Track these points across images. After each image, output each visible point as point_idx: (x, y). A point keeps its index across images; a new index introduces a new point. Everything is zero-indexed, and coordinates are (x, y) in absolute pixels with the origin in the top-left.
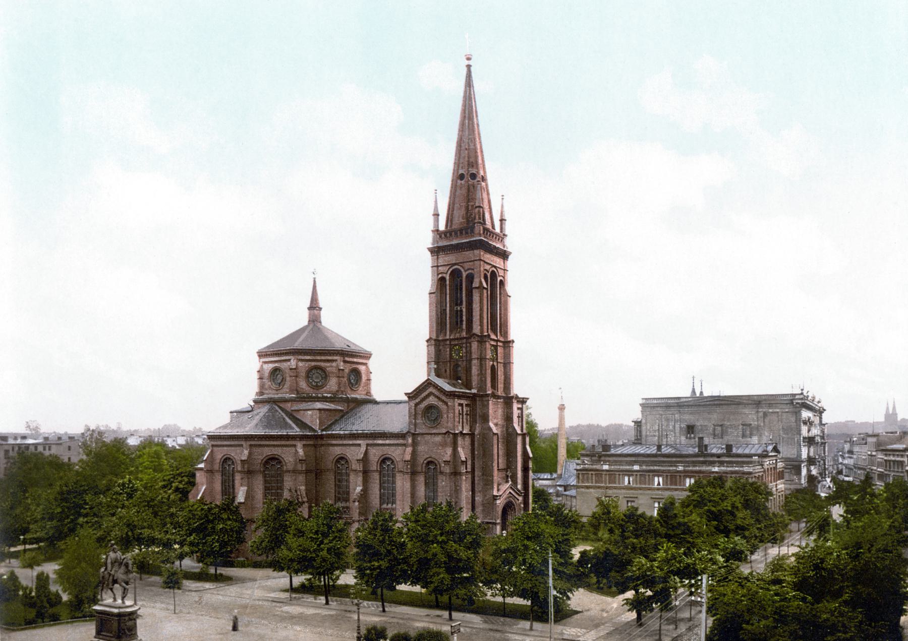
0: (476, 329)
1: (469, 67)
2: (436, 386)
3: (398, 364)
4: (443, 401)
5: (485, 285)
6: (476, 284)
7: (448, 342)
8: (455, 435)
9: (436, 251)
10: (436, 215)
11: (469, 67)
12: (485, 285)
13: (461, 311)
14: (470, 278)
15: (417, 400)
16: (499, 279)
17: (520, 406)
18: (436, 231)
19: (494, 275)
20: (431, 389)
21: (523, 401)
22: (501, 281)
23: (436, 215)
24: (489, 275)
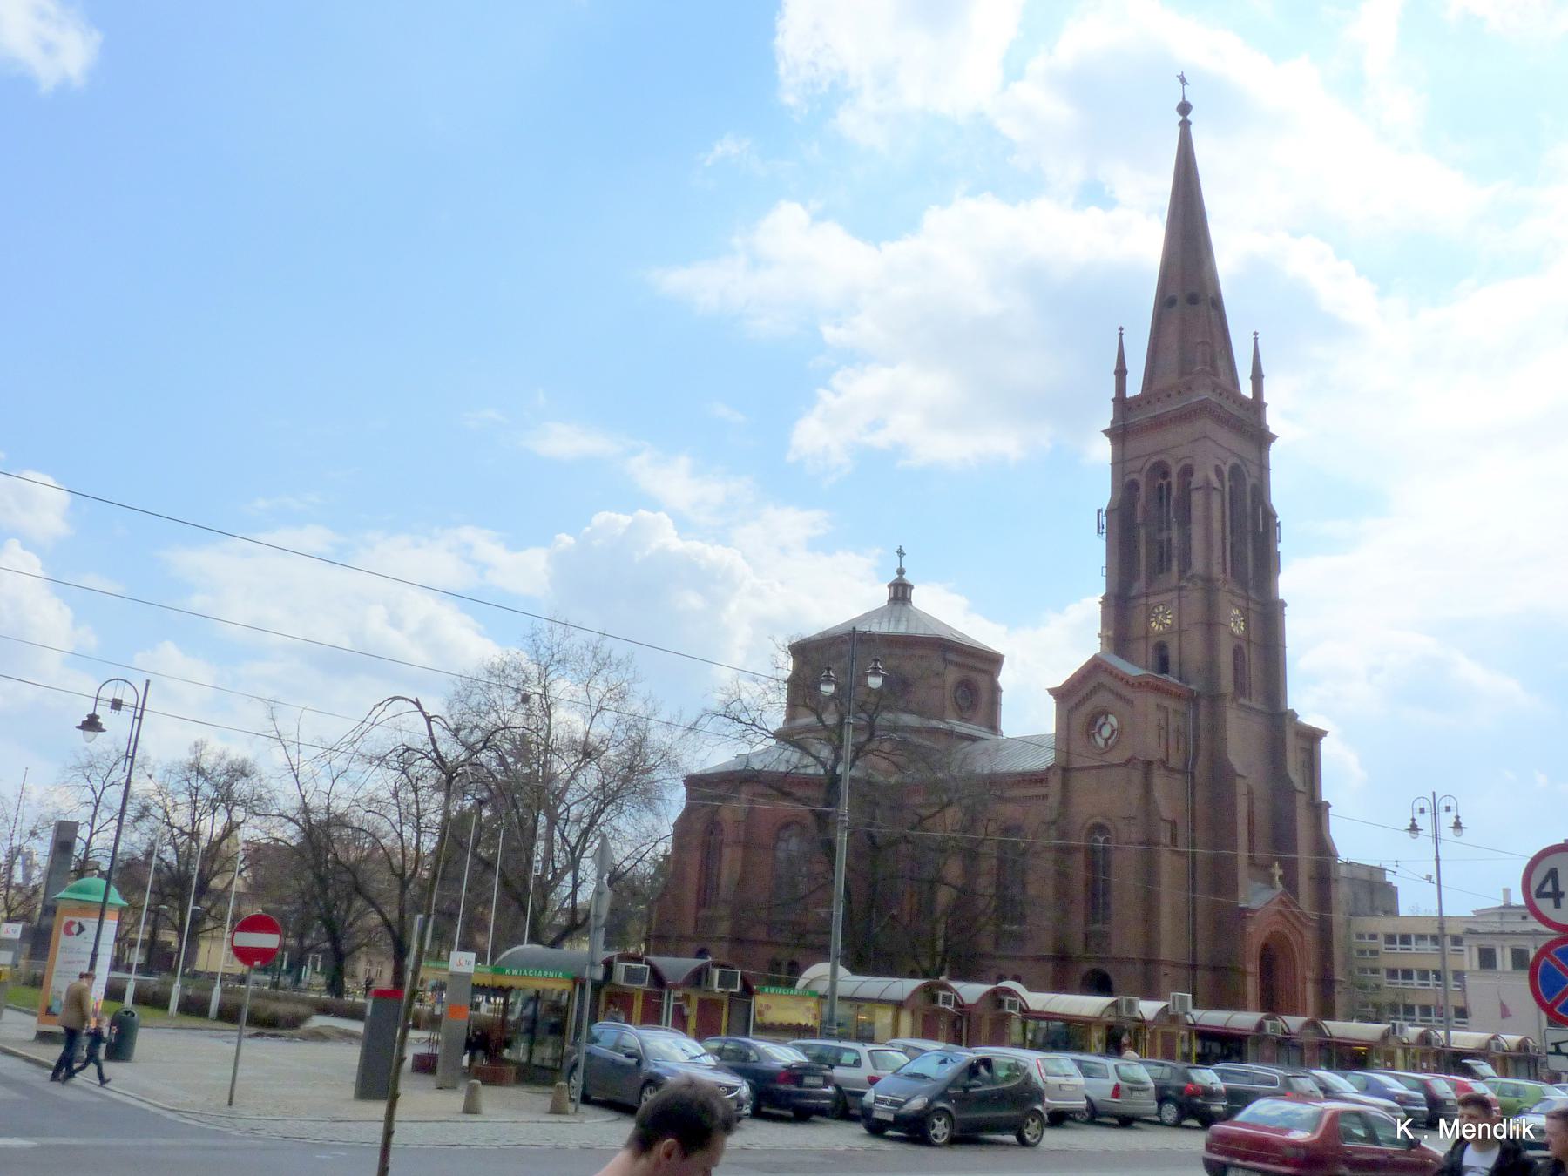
0: (1198, 566)
1: (1185, 125)
2: (1111, 672)
3: (1042, 638)
4: (1125, 700)
5: (1216, 483)
6: (1197, 480)
7: (1143, 601)
8: (1148, 764)
9: (1119, 434)
10: (1121, 372)
11: (1185, 125)
12: (1216, 483)
13: (1169, 540)
14: (1187, 472)
15: (1075, 700)
16: (1250, 482)
17: (1307, 746)
18: (1121, 402)
19: (1236, 472)
20: (1104, 679)
21: (1313, 737)
22: (1254, 487)
23: (1121, 372)
24: (1226, 469)
